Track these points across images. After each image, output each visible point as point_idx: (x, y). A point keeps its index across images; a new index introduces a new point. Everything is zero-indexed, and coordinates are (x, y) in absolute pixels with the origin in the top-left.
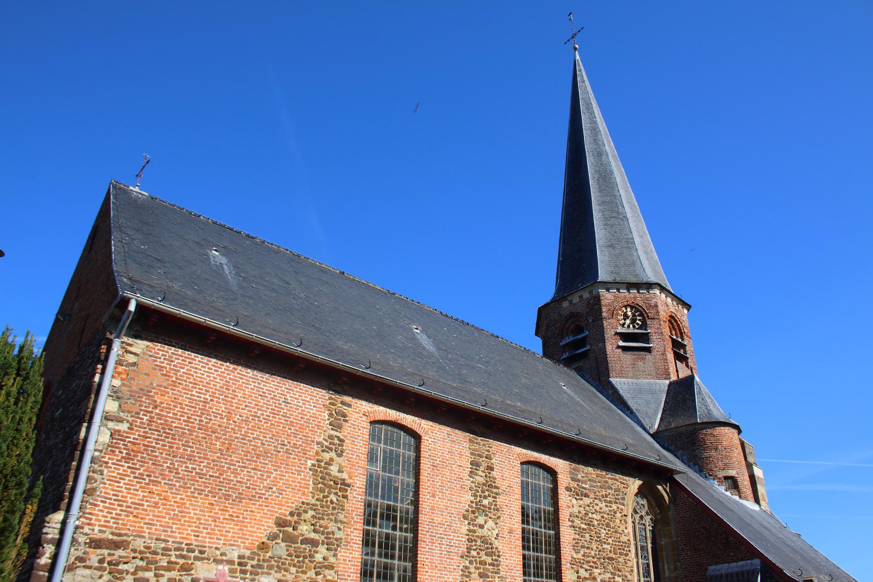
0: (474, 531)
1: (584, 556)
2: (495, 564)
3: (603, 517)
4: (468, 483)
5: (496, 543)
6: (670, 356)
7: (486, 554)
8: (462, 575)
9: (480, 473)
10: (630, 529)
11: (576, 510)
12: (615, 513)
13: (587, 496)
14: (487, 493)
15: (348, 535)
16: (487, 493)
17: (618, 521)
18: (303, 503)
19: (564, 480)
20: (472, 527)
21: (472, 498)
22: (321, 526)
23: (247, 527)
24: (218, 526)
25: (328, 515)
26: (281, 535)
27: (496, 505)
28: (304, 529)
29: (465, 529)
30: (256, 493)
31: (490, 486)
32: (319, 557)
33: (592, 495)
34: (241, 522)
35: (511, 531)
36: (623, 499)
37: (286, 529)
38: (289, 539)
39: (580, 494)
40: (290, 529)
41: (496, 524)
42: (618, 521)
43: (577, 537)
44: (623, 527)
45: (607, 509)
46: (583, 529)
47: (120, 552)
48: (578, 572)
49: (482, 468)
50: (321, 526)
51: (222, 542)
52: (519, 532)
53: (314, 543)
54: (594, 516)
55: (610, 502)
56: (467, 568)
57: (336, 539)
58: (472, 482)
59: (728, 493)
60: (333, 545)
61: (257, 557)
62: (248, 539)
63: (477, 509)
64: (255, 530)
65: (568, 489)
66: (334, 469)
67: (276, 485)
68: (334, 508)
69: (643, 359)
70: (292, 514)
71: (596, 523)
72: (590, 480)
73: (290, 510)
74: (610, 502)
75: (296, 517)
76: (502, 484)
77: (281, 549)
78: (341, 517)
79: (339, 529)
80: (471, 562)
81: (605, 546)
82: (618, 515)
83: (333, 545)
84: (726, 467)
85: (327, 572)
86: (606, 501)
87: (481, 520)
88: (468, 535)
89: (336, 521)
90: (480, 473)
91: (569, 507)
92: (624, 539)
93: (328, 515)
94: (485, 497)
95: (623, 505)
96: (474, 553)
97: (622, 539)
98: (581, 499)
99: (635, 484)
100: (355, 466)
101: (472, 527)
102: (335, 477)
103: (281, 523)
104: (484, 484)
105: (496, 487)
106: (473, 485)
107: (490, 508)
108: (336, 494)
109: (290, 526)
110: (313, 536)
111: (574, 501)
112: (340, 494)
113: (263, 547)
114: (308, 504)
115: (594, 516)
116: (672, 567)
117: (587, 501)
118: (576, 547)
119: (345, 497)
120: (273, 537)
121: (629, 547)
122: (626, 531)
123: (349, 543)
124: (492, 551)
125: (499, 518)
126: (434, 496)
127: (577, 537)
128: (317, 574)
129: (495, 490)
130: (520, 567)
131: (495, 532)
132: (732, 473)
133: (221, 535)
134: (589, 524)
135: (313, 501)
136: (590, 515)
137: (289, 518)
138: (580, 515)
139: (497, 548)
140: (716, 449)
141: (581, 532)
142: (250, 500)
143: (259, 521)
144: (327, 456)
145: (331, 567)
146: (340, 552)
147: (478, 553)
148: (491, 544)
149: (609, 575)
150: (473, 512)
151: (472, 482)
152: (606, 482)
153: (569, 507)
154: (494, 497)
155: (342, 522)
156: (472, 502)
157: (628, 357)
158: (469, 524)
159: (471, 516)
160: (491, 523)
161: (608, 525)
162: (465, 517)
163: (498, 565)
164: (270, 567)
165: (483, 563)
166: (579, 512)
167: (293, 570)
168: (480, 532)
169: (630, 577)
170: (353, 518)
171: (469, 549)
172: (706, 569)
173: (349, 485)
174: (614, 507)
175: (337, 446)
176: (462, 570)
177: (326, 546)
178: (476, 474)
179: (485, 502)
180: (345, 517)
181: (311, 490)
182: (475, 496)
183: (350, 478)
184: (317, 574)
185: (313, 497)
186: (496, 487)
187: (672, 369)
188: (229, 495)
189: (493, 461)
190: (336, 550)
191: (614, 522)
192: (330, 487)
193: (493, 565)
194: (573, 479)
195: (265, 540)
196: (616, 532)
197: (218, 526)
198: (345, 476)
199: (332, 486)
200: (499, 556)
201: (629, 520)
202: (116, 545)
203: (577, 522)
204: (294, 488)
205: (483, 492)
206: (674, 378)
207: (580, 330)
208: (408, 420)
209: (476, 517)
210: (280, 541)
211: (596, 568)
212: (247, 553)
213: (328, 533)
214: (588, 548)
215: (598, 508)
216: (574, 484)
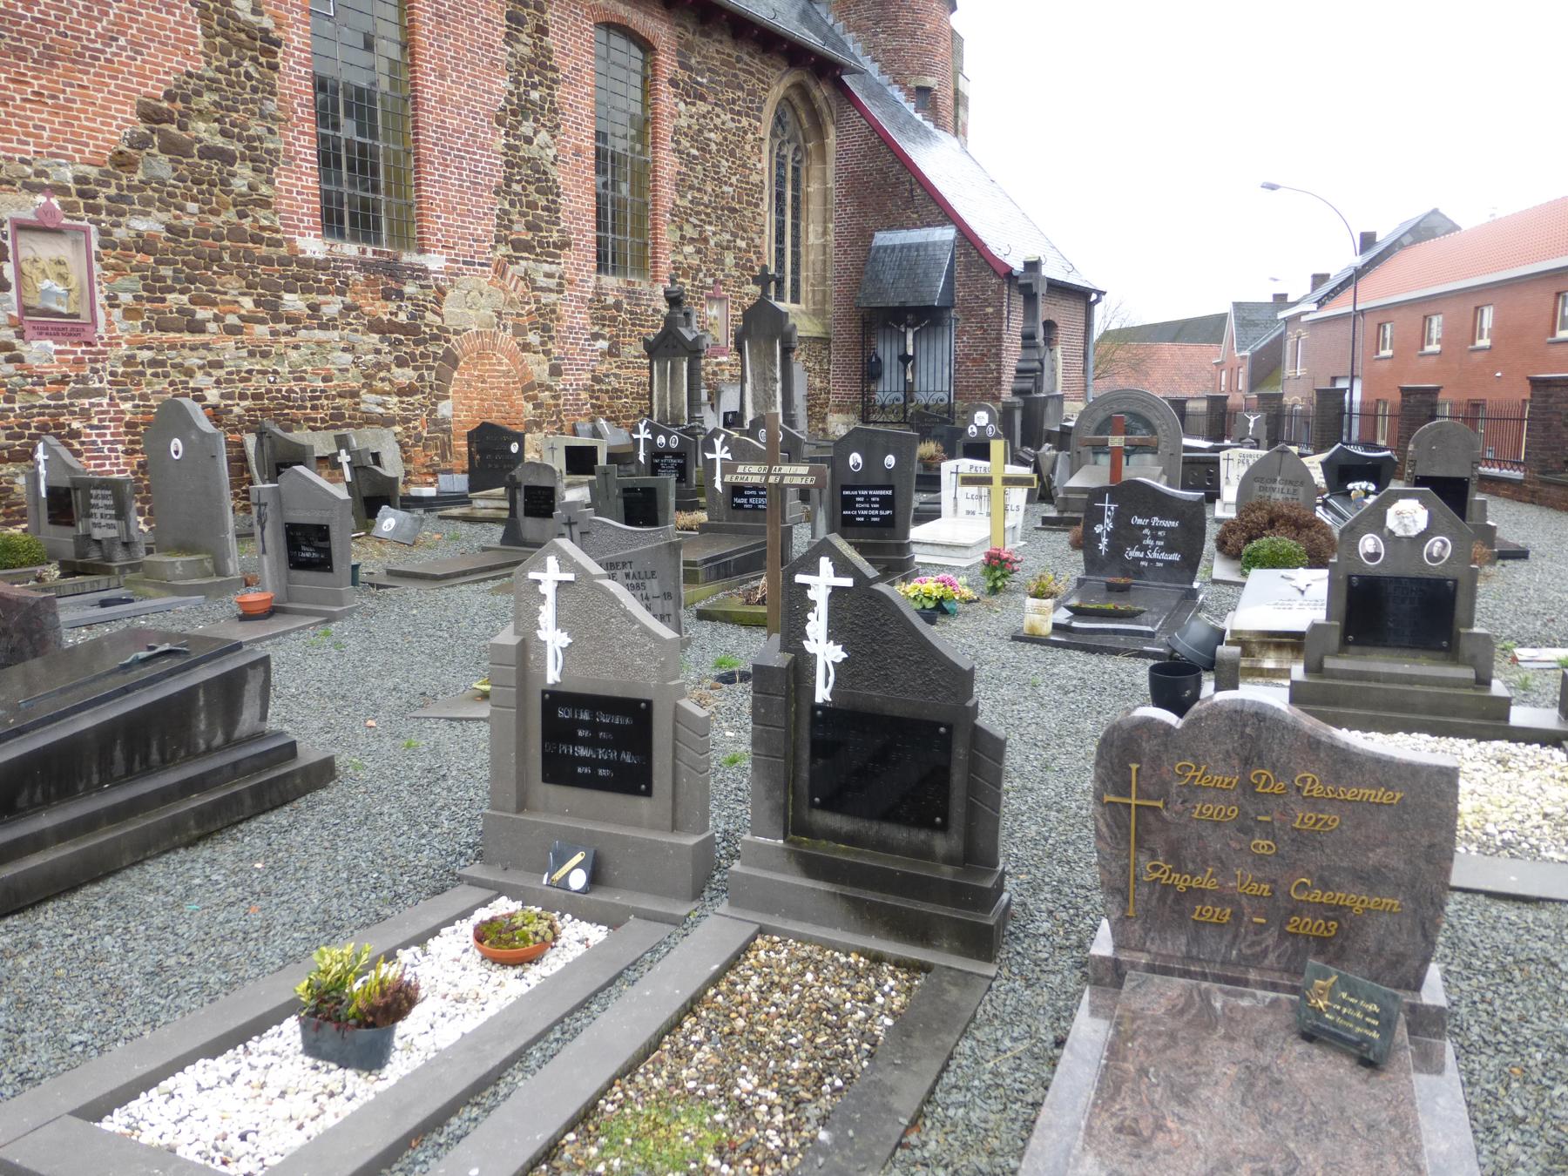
0: (516, 148)
1: (691, 202)
2: (552, 209)
3: (725, 139)
4: (505, 57)
5: (554, 172)
7: (538, 191)
8: (499, 225)
9: (524, 37)
10: (765, 164)
11: (683, 122)
12: (745, 133)
13: (702, 98)
14: (536, 79)
15: (288, 143)
16: (536, 79)
17: (748, 147)
18: (190, 75)
19: (667, 64)
20: (512, 141)
21: (512, 87)
22: (233, 124)
23: (78, 119)
24: (14, 115)
25: (245, 102)
26: (155, 139)
27: (552, 103)
28: (202, 129)
30: (83, 47)
31: (541, 63)
32: (239, 185)
33: (711, 99)
34: (63, 108)
35: (578, 152)
36: (760, 109)
37: (164, 126)
38: (173, 147)
39: (692, 94)
40: (173, 128)
41: (554, 137)
42: (748, 147)
43: (684, 169)
44: (754, 159)
45: (732, 125)
46: (695, 157)
48: (681, 229)
49: (528, 29)
50: (233, 124)
51: (32, 148)
52: (591, 154)
53: (227, 158)
54: (712, 135)
55: (739, 113)
56: (506, 212)
57: (268, 152)
58: (511, 55)
59: (918, 117)
60: (263, 162)
61: (114, 182)
62: (87, 145)
63: (521, 109)
64: (97, 125)
65: (673, 83)
67: (124, 34)
68: (254, 90)
70: (169, 96)
71: (714, 147)
72: (709, 70)
73: (165, 88)
74: (739, 113)
75: (179, 105)
76: (565, 65)
77: (162, 166)
78: (271, 107)
79: (270, 131)
80: (512, 204)
81: (725, 188)
82: (750, 136)
83: (263, 162)
84: (925, 69)
85: (260, 212)
86: (732, 111)
88: (505, 154)
89: (263, 117)
90: (524, 37)
91: (673, 116)
92: (755, 178)
93: (245, 102)
94: (534, 86)
95: (759, 120)
96: (516, 187)
97: (751, 179)
98: (694, 104)
101: (512, 141)
102: (247, 22)
103: (151, 115)
104: (531, 61)
105: (555, 70)
106: (512, 60)
107: (542, 108)
108: (254, 59)
109: (172, 122)
110: (219, 141)
111: (682, 106)
112: (262, 60)
113: (122, 162)
114: (200, 78)
115: (712, 135)
116: (820, 230)
117: (703, 107)
118: (681, 184)
119: (274, 67)
120: (141, 143)
121: (761, 192)
122: (759, 166)
123: (294, 159)
124: (548, 188)
125: (557, 126)
126: (442, 77)
127: (684, 169)
128: (242, 215)
129: (550, 74)
130: (591, 216)
131: (551, 152)
132: (930, 81)
133: (28, 134)
134: (703, 149)
135: (210, 74)
136: (706, 134)
137: (165, 105)
138: (691, 133)
139: (554, 181)
140: (913, 35)
141: (690, 161)
142: (74, 62)
143: (102, 107)
145: (265, 203)
146: (279, 175)
147: (524, 188)
148: (545, 173)
149: (728, 237)
150: (514, 113)
151: (511, 55)
152: (735, 76)
153: (673, 116)
154: (550, 88)
155: (275, 119)
156: (511, 93)
158: (507, 134)
159: (510, 119)
160: (543, 136)
161: (732, 153)
162: (500, 122)
163: (557, 211)
164: (147, 202)
165: (532, 205)
166: (689, 127)
167: (192, 207)
169: (757, 241)
170: (295, 112)
171: (509, 180)
172: (872, 236)
173: (278, 44)
174: (745, 122)
176: (498, 217)
177: (250, 164)
178: (518, 41)
179: (535, 95)
180: (280, 108)
181: (201, 47)
182: (516, 82)
183: (279, 26)
184: (242, 215)
185: (209, 64)
186: (555, 70)
188: (24, 50)
189: (548, 16)
190: (270, 172)
191: (743, 148)
192: (239, 44)
193: (545, 209)
194: (683, 66)
195: (122, 148)
196: (744, 166)
197: (14, 115)
198: (267, 22)
200: (558, 195)
201: (766, 147)
203: (685, 143)
205: (530, 75)
209: (520, 123)
210: (155, 151)
211: (710, 223)
212: (93, 172)
213: (251, 139)
214: (699, 190)
215: (718, 121)
216: (682, 75)
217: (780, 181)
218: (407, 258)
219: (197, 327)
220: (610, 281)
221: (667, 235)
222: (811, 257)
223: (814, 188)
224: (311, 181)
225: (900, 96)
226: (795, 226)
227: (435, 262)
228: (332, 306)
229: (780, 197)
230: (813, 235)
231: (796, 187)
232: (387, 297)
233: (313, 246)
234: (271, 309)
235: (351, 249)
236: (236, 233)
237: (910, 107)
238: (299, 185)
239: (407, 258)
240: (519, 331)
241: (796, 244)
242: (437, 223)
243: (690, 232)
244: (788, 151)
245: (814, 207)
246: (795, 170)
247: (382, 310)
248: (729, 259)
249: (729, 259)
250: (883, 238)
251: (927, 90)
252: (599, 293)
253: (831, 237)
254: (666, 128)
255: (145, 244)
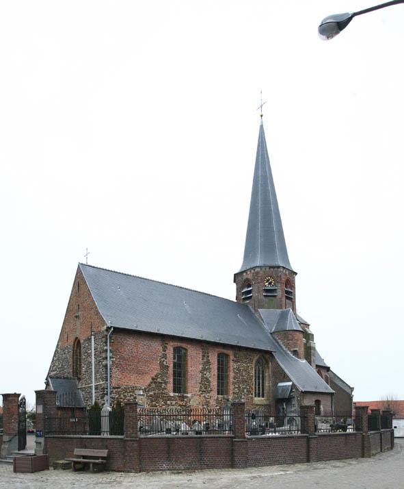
6: (284, 299)
19: (232, 357)
29: (200, 375)
31: (208, 362)
38: (155, 383)
47: (119, 390)
63: (204, 369)
66: (165, 363)
69: (272, 300)
77: (153, 385)
83: (166, 383)
87: (205, 373)
99: (256, 358)
100: (170, 361)
103: (153, 379)
113: (149, 385)
118: (234, 378)
120: (151, 383)
124: (209, 382)
132: (296, 349)
144: (162, 360)
157: (267, 300)
168: (205, 376)
175: (165, 356)
187: (284, 304)
199: (164, 367)
202: (119, 388)
204: (155, 369)
206: (284, 310)
207: (249, 286)
208: (184, 345)
217: (259, 374)
218: (186, 395)
219: (156, 406)
220: (220, 396)
221: (231, 387)
222: (266, 388)
223: (267, 374)
224: (172, 385)
225: (289, 353)
226: (263, 383)
227: (189, 395)
228: (174, 403)
229: (259, 377)
230: (267, 384)
231: (263, 374)
232: (182, 401)
233: (172, 394)
234: (166, 404)
235: (177, 394)
236: (162, 393)
237: (292, 355)
238: (170, 386)
239: (186, 395)
240: (203, 405)
241: (263, 385)
242: (189, 389)
243: (236, 386)
244: (261, 368)
245: (267, 379)
246: (263, 372)
247: (181, 403)
248: (245, 390)
249: (245, 390)
250: (280, 384)
251: (296, 351)
252: (218, 398)
253: (271, 384)
254: (232, 369)
255: (151, 396)
